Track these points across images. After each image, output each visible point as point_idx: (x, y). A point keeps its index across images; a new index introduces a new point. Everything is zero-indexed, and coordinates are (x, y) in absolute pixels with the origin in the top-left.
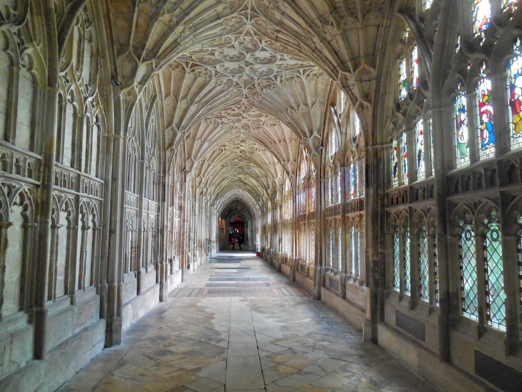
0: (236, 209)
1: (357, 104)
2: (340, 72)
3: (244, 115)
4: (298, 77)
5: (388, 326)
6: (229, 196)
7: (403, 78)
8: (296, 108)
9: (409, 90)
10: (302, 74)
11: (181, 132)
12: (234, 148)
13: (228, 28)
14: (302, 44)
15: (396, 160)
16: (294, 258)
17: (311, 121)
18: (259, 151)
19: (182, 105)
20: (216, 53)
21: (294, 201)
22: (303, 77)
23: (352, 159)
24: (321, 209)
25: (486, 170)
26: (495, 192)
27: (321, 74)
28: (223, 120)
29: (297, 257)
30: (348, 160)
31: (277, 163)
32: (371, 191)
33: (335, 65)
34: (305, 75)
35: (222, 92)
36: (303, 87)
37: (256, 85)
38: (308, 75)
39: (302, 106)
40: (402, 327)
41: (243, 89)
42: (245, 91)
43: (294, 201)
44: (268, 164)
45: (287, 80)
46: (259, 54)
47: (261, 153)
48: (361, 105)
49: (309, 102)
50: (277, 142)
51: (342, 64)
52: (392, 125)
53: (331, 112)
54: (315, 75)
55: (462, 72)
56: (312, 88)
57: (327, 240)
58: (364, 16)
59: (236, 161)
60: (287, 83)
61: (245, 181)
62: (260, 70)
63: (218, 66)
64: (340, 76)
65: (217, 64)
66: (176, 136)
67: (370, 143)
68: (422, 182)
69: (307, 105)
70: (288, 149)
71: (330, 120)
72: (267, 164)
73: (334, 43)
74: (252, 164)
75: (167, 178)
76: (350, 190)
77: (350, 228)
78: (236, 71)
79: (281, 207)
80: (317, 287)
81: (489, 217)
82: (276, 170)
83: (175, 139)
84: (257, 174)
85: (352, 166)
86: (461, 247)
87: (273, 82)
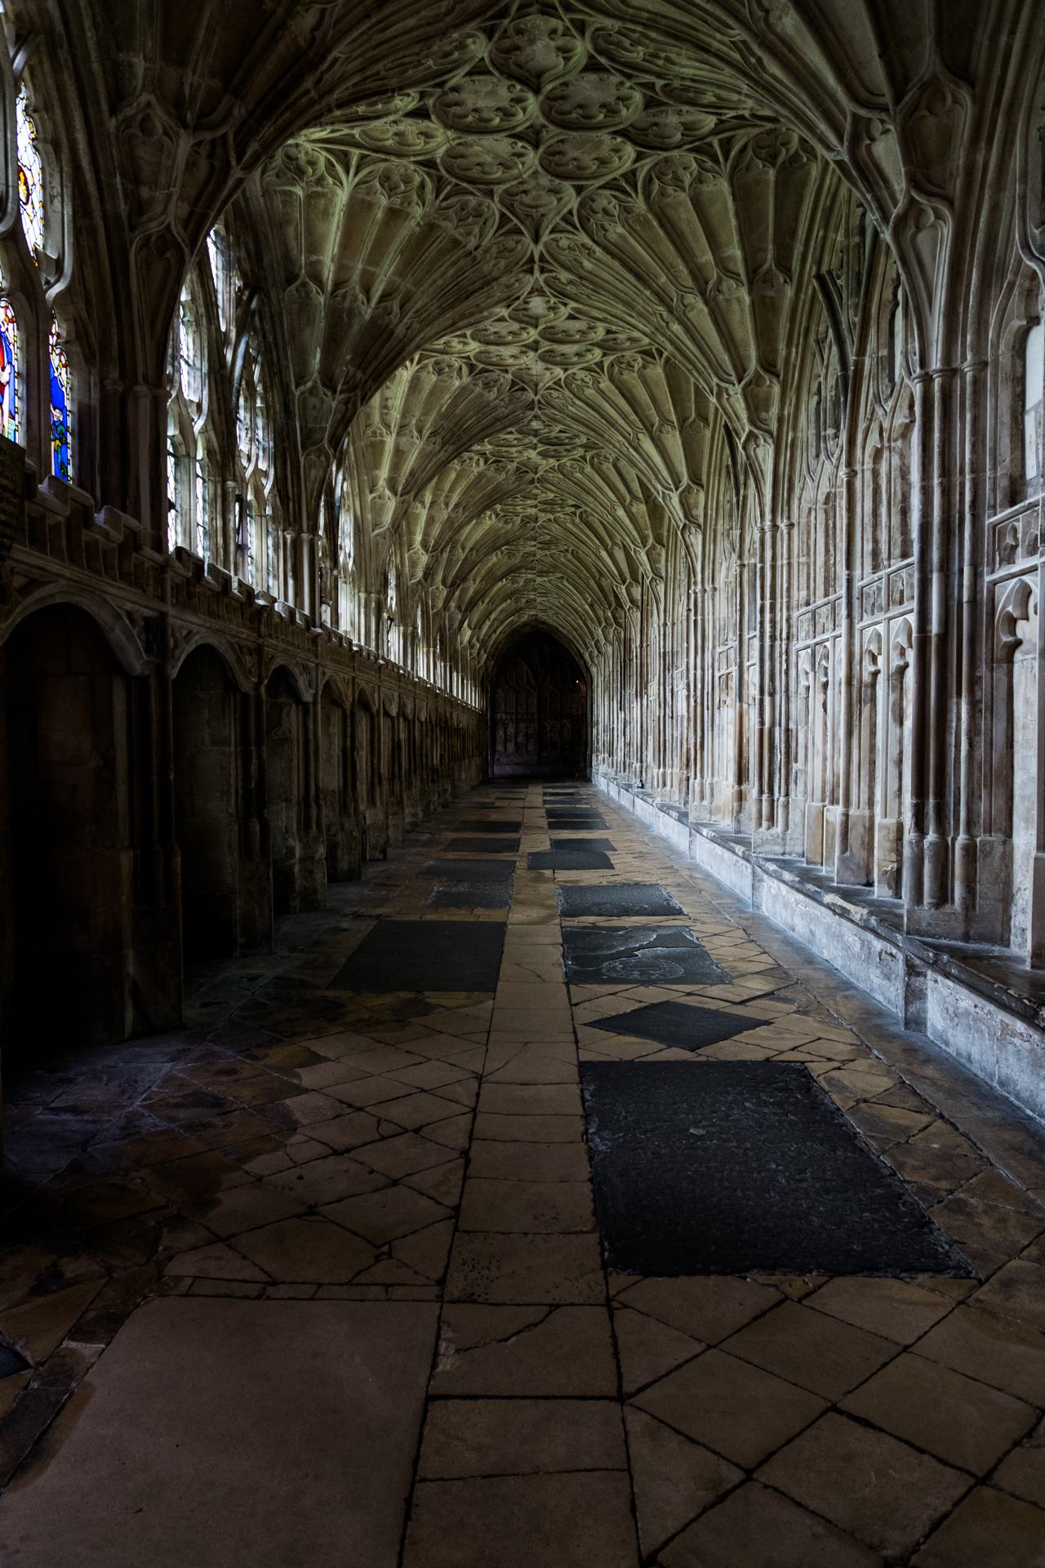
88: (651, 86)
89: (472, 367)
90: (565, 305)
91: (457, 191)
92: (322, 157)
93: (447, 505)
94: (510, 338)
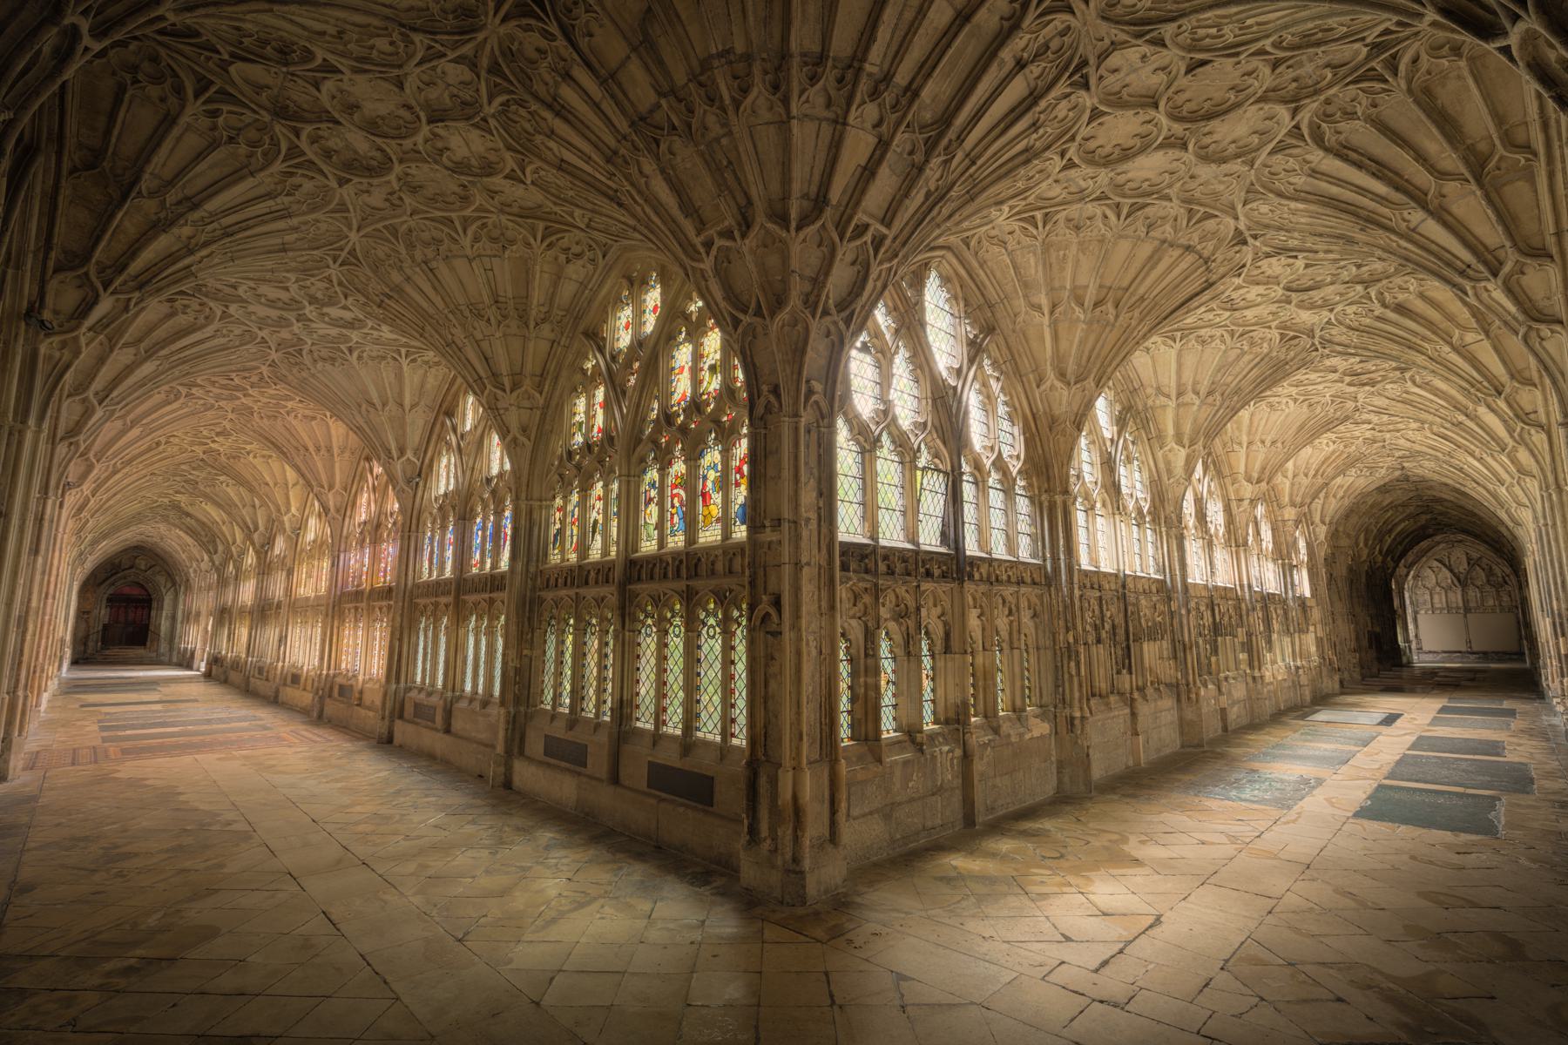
0: (131, 567)
1: (509, 438)
2: (489, 387)
4: (395, 359)
5: (530, 760)
6: (129, 536)
7: (580, 417)
8: (379, 408)
9: (586, 436)
12: (192, 444)
13: (293, 264)
14: (428, 328)
15: (558, 526)
16: (325, 672)
17: (404, 431)
19: (121, 357)
21: (334, 564)
22: (404, 362)
23: (479, 510)
24: (406, 585)
25: (674, 559)
26: (681, 585)
27: (438, 364)
28: (194, 390)
29: (332, 672)
30: (472, 510)
31: (294, 485)
32: (519, 566)
33: (482, 374)
35: (224, 348)
36: (399, 376)
37: (304, 353)
38: (414, 361)
39: (391, 405)
40: (552, 756)
41: (273, 352)
42: (274, 356)
43: (333, 565)
44: (271, 484)
45: (372, 358)
46: (334, 312)
47: (258, 462)
48: (515, 440)
49: (407, 402)
50: (312, 449)
51: (495, 375)
52: (557, 477)
53: (443, 424)
54: (427, 363)
55: (656, 443)
56: (417, 379)
57: (413, 639)
58: (537, 324)
59: (183, 467)
60: (370, 362)
61: (190, 509)
62: (321, 332)
64: (486, 392)
66: (90, 417)
67: (523, 496)
68: (597, 563)
69: (402, 405)
70: (333, 467)
71: (439, 436)
72: (267, 484)
73: (485, 345)
74: (222, 478)
75: (50, 502)
76: (471, 558)
77: (466, 619)
78: (270, 321)
79: (290, 573)
80: (387, 721)
81: (672, 610)
82: (288, 498)
83: (86, 423)
84: (230, 499)
85: (478, 520)
86: (639, 644)
88: (1261, 52)
89: (1232, 333)
90: (1296, 257)
91: (1136, 208)
92: (1016, 225)
93: (1263, 442)
94: (1259, 299)
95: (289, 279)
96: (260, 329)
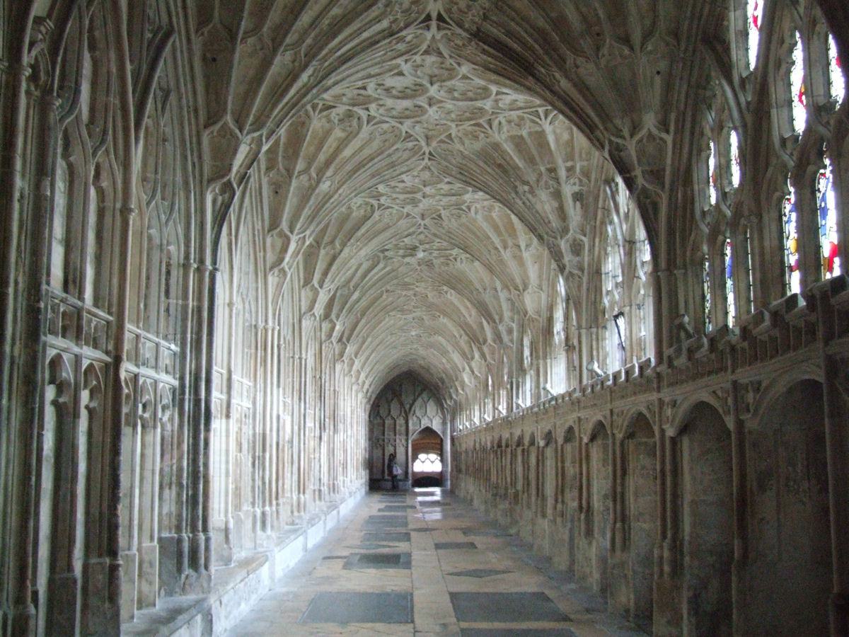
3: (428, 190)
10: (543, 117)
11: (297, 237)
18: (462, 262)
20: (371, 86)
34: (549, 119)
63: (373, 107)
65: (370, 102)
87: (483, 130)
95: (399, 66)
96: (401, 123)
